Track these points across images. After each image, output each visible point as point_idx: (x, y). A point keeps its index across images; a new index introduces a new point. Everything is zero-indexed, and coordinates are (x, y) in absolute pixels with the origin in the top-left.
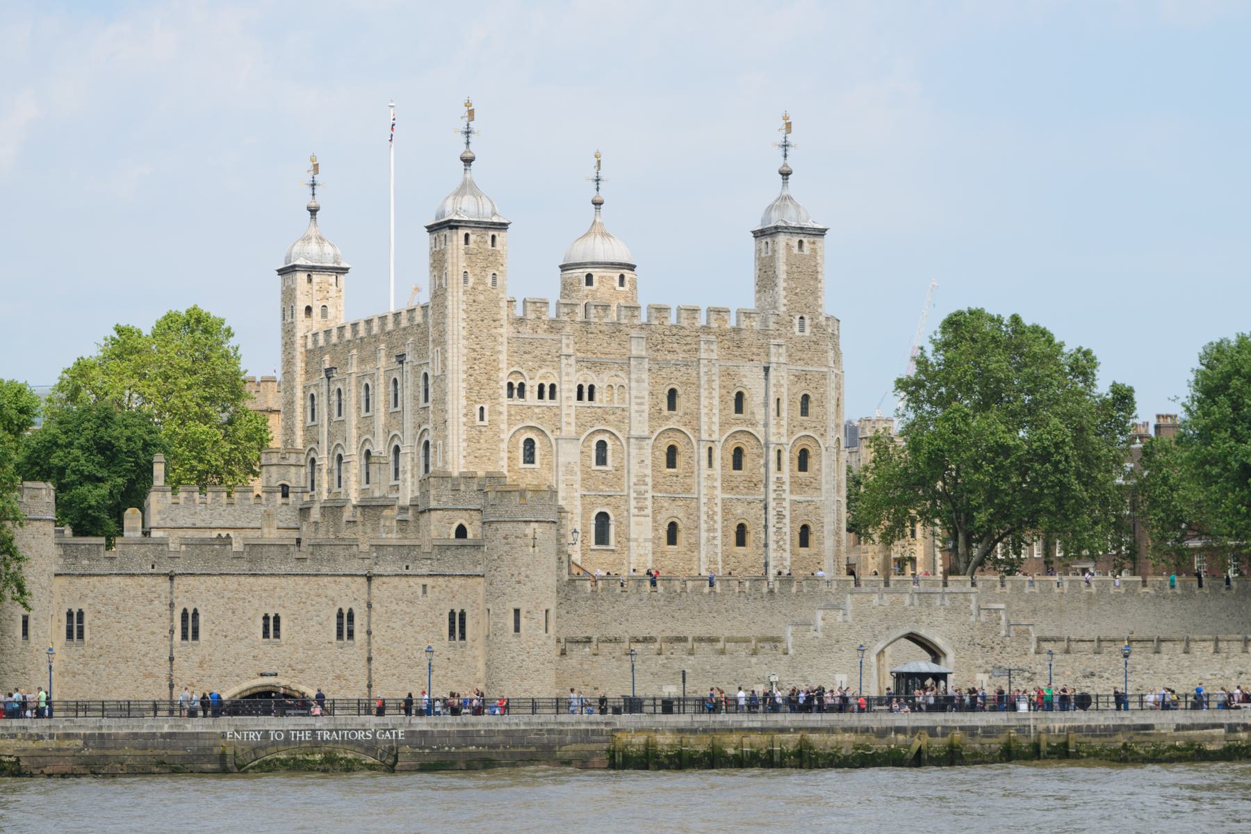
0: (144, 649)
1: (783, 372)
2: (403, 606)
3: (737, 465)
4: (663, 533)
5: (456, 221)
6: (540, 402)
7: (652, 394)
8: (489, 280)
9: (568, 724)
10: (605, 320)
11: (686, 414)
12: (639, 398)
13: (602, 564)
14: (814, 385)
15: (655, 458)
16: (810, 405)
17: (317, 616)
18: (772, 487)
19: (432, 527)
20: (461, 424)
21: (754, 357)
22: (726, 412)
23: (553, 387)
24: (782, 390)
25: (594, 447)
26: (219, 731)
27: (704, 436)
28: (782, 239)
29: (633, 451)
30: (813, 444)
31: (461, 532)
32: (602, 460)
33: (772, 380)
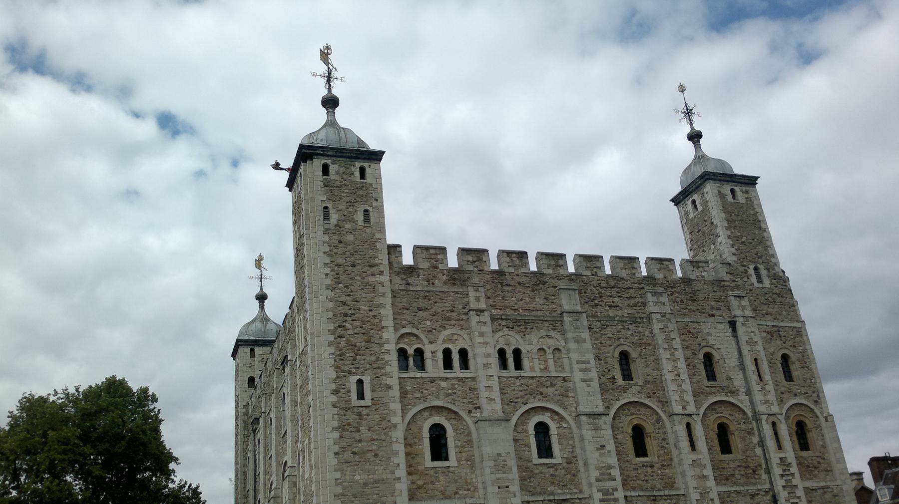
1: (753, 325)
3: (726, 448)
6: (448, 374)
7: (597, 358)
8: (360, 217)
10: (523, 270)
14: (791, 343)
15: (618, 443)
16: (792, 367)
18: (777, 471)
20: (330, 406)
25: (532, 432)
27: (678, 409)
30: (809, 415)
32: (545, 450)
33: (743, 338)
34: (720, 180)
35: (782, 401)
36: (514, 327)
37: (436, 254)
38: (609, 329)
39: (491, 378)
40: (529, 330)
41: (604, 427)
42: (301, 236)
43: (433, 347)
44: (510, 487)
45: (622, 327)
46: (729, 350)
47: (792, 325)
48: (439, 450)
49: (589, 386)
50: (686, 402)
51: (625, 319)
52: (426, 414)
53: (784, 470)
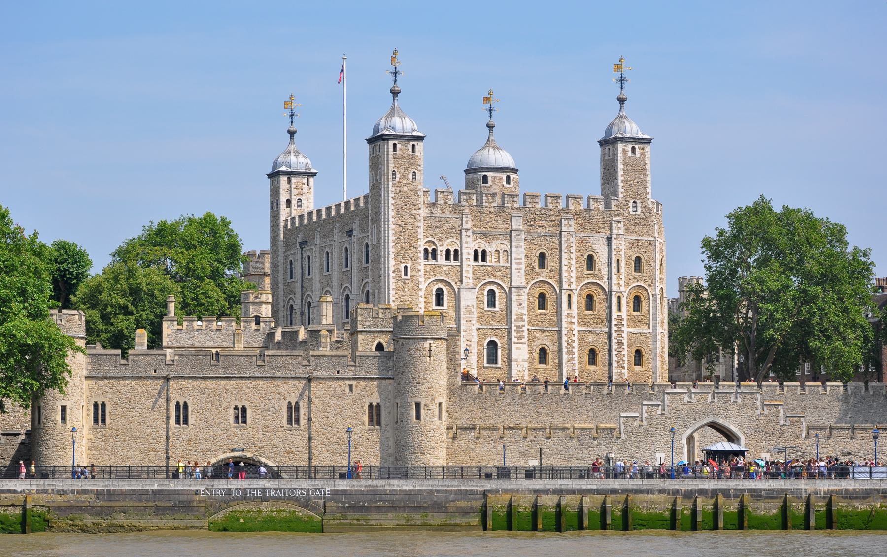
0: (149, 431)
2: (334, 400)
4: (536, 356)
5: (387, 135)
6: (448, 263)
7: (527, 256)
8: (410, 176)
9: (452, 486)
10: (494, 204)
11: (551, 270)
12: (518, 259)
14: (644, 250)
15: (530, 302)
17: (273, 407)
18: (614, 322)
19: (359, 344)
22: (581, 269)
23: (456, 251)
24: (621, 253)
25: (486, 294)
26: (194, 488)
27: (565, 286)
28: (620, 146)
29: (514, 297)
31: (380, 347)
32: (491, 303)
33: (614, 247)
41: (523, 294)
42: (376, 180)
46: (603, 253)
48: (439, 300)
49: (519, 272)
51: (546, 234)
52: (435, 283)
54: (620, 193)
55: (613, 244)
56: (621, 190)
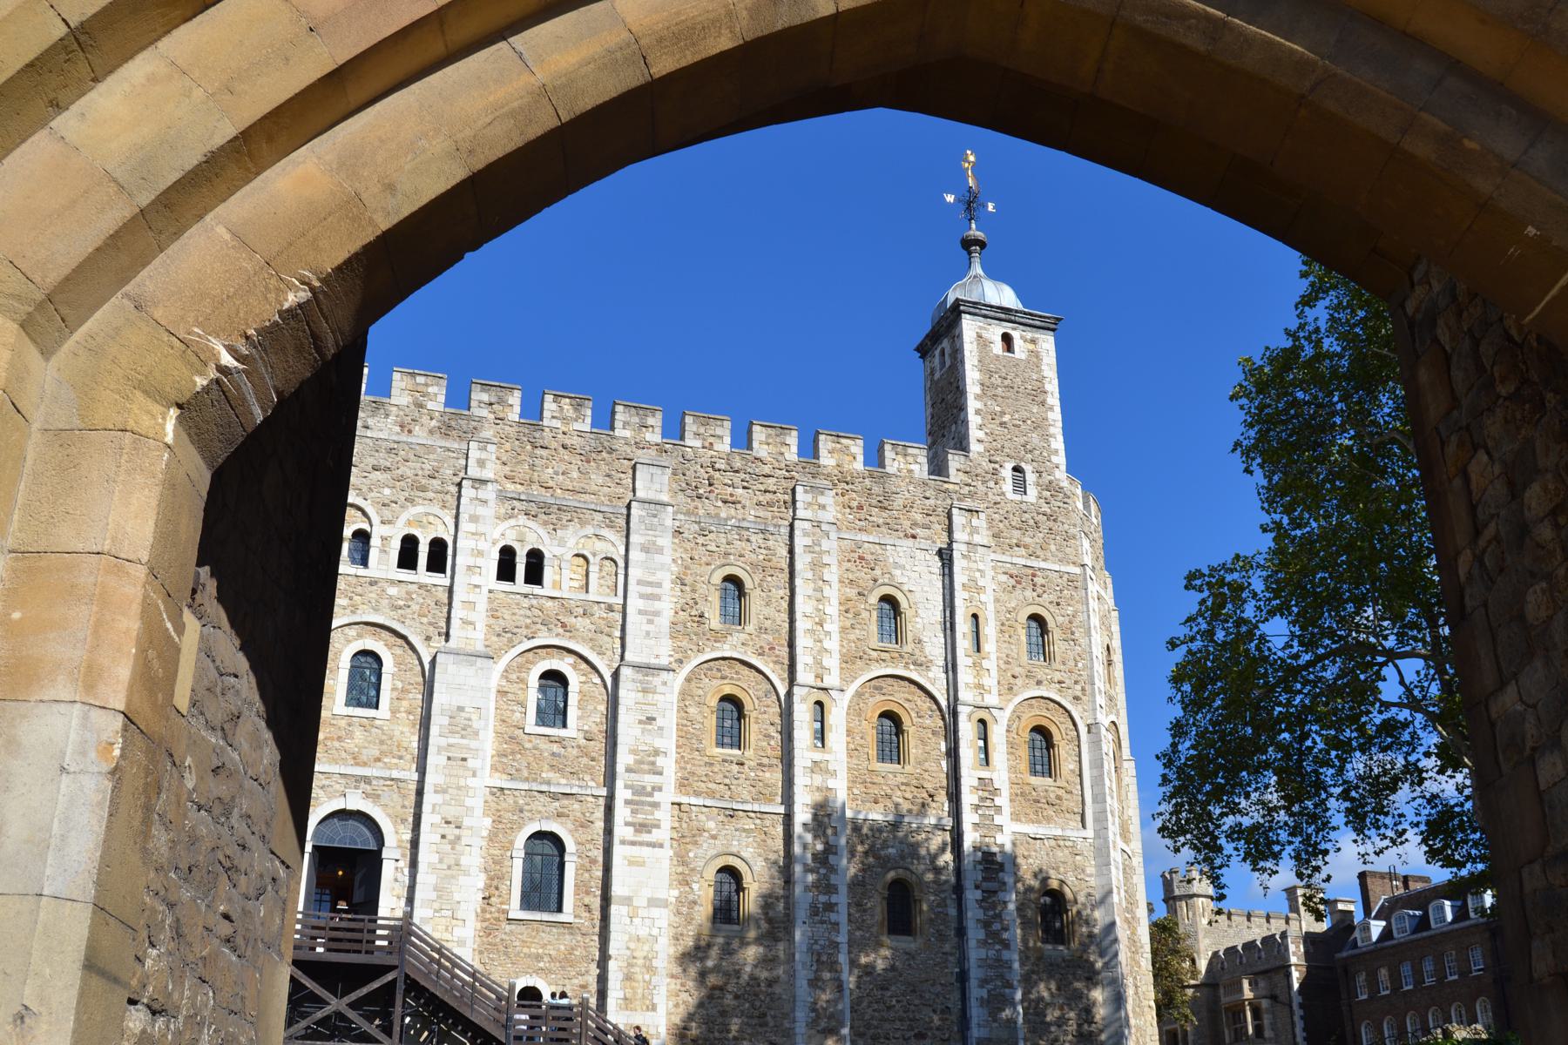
6: (405, 575)
10: (578, 426)
12: (650, 584)
13: (539, 958)
14: (1053, 598)
18: (968, 798)
21: (918, 531)
23: (438, 547)
24: (983, 598)
27: (803, 676)
28: (969, 327)
29: (627, 695)
32: (554, 713)
33: (959, 578)
34: (985, 316)
35: (1010, 689)
36: (540, 516)
37: (426, 385)
38: (711, 536)
39: (478, 590)
40: (564, 522)
41: (660, 689)
43: (385, 530)
44: (469, 760)
45: (737, 537)
47: (1063, 569)
49: (650, 622)
50: (823, 668)
51: (745, 524)
52: (352, 632)
53: (982, 799)
54: (972, 440)
55: (956, 569)
56: (974, 433)
